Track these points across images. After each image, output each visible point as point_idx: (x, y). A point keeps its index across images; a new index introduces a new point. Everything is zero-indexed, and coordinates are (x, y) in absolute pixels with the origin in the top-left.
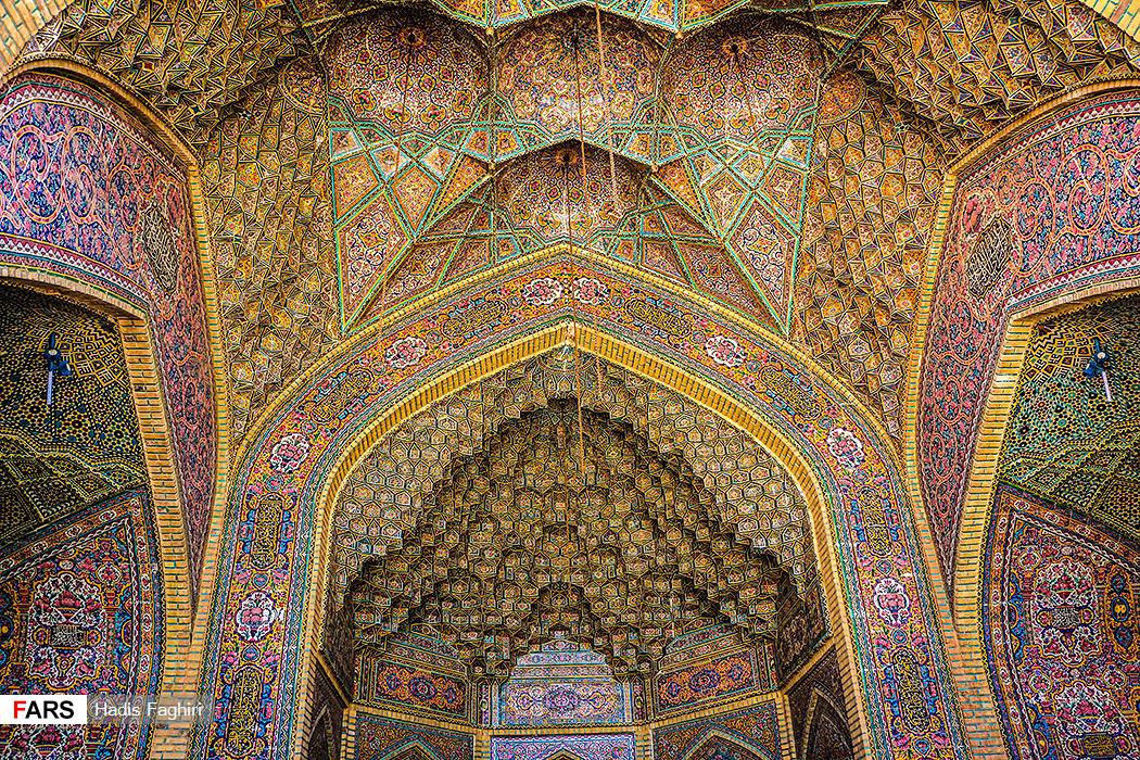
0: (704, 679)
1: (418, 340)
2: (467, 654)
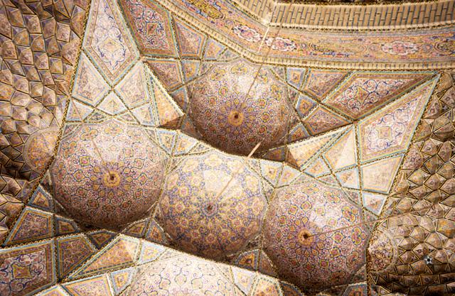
1: (387, 51)
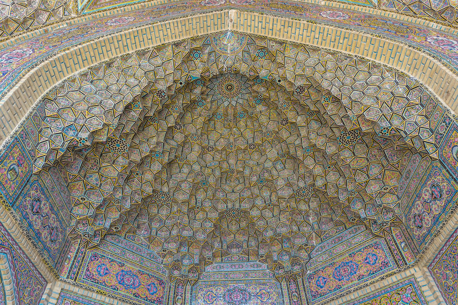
0: (345, 270)
2: (169, 260)
